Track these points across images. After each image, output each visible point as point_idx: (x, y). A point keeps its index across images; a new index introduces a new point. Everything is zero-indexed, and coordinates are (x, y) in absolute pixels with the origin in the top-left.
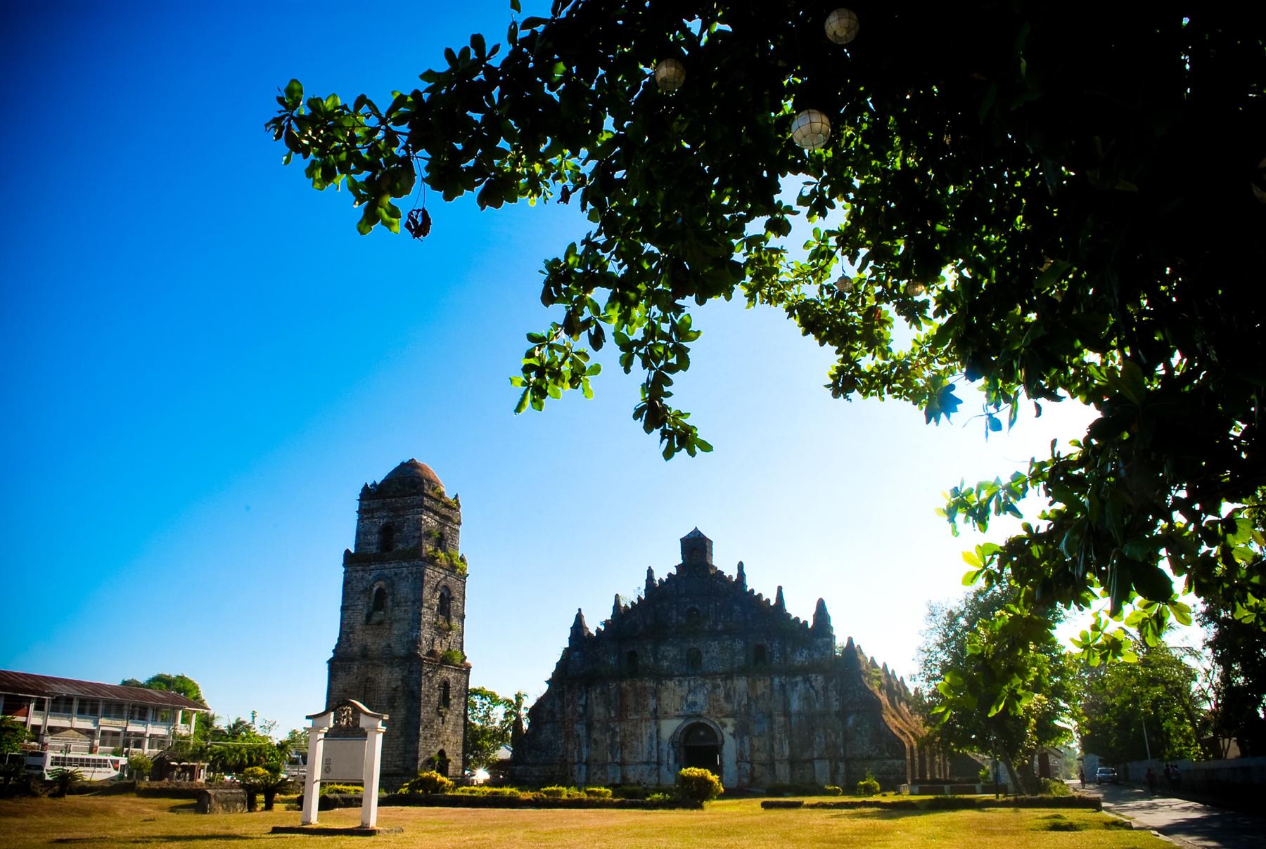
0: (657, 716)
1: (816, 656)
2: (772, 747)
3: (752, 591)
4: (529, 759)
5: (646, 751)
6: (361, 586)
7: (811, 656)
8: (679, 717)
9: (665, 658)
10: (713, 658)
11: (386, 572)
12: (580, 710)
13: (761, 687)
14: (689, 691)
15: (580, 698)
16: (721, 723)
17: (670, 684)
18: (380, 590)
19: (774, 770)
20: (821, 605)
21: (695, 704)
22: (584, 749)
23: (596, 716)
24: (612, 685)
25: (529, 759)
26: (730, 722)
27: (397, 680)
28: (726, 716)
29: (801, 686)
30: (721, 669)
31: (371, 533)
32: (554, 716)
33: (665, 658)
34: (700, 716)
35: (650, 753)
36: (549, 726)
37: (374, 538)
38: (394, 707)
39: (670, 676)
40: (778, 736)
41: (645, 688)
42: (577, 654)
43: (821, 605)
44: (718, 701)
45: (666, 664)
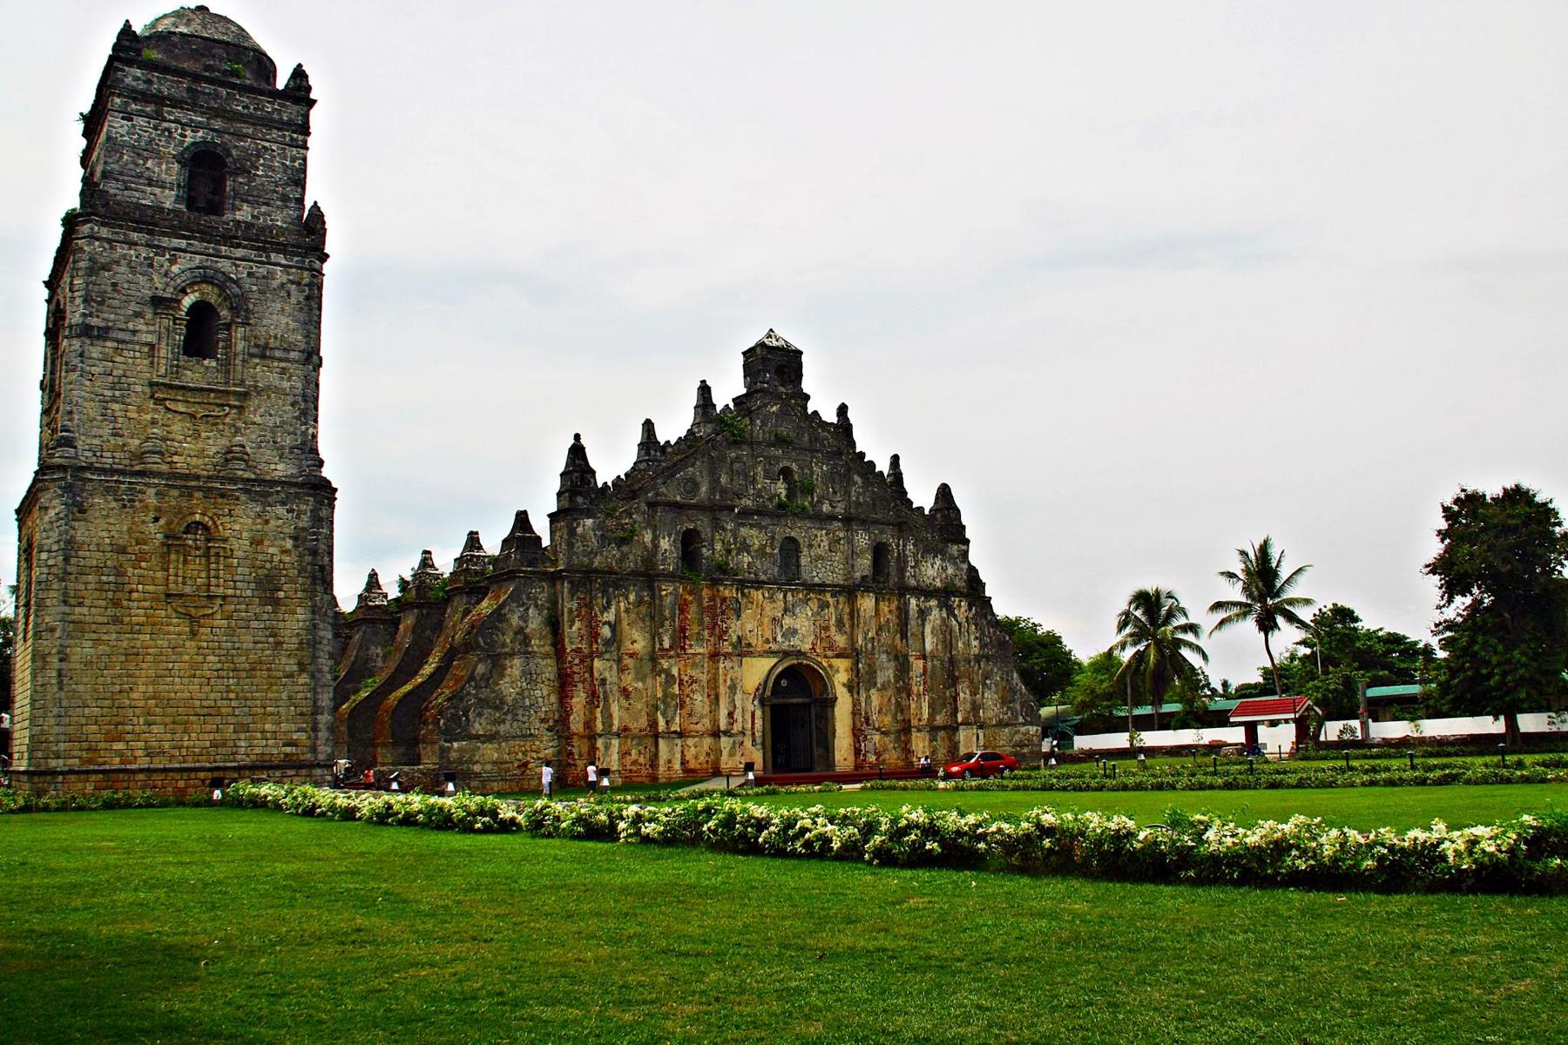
0: (743, 650)
1: (950, 571)
2: (900, 708)
3: (862, 455)
4: (478, 727)
5: (723, 712)
6: (145, 287)
7: (944, 569)
8: (769, 653)
9: (745, 547)
10: (820, 557)
11: (224, 265)
12: (606, 631)
13: (884, 607)
14: (786, 610)
15: (606, 608)
16: (831, 666)
17: (757, 595)
18: (201, 311)
19: (908, 742)
20: (944, 493)
21: (795, 632)
22: (615, 708)
23: (628, 646)
24: (667, 589)
25: (478, 727)
26: (842, 664)
27: (279, 533)
28: (838, 656)
29: (935, 612)
30: (830, 579)
31: (159, 156)
32: (526, 640)
33: (745, 547)
34: (800, 653)
35: (731, 715)
36: (517, 662)
37: (171, 172)
38: (276, 603)
39: (758, 584)
40: (915, 689)
41: (724, 600)
42: (589, 522)
43: (944, 493)
44: (827, 628)
45: (747, 559)
